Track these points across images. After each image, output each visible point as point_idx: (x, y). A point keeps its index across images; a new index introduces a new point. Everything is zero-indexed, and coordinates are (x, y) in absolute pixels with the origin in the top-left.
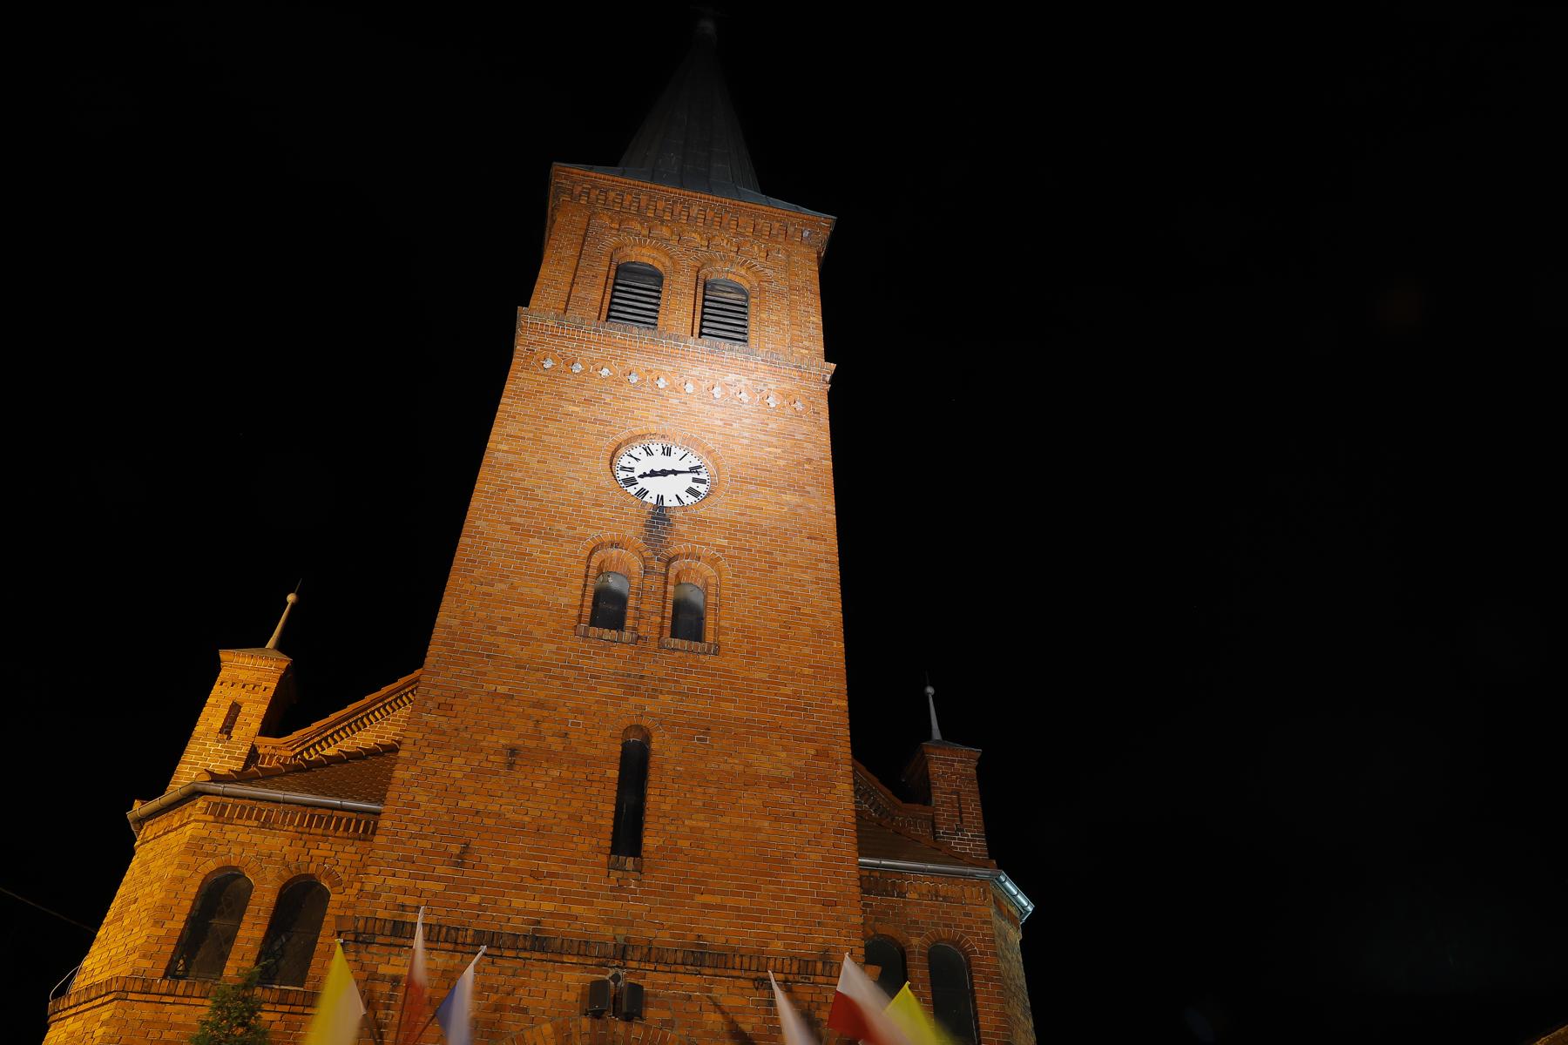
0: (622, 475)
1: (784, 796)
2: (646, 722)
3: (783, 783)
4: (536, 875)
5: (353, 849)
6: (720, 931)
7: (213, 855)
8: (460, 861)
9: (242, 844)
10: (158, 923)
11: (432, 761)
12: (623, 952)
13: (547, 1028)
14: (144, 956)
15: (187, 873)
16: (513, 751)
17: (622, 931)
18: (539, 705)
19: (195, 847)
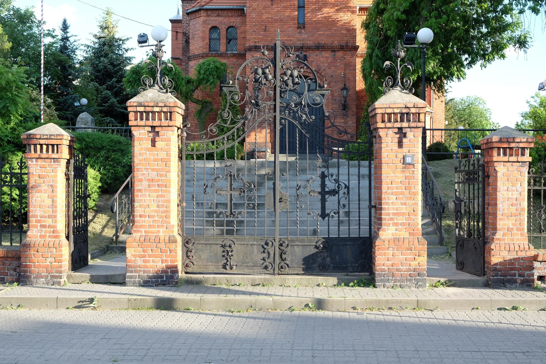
5: (239, 18)
6: (323, 40)
7: (209, 24)
8: (265, 30)
9: (214, 20)
10: (203, 41)
12: (302, 48)
14: (204, 49)
15: (205, 29)
19: (204, 22)
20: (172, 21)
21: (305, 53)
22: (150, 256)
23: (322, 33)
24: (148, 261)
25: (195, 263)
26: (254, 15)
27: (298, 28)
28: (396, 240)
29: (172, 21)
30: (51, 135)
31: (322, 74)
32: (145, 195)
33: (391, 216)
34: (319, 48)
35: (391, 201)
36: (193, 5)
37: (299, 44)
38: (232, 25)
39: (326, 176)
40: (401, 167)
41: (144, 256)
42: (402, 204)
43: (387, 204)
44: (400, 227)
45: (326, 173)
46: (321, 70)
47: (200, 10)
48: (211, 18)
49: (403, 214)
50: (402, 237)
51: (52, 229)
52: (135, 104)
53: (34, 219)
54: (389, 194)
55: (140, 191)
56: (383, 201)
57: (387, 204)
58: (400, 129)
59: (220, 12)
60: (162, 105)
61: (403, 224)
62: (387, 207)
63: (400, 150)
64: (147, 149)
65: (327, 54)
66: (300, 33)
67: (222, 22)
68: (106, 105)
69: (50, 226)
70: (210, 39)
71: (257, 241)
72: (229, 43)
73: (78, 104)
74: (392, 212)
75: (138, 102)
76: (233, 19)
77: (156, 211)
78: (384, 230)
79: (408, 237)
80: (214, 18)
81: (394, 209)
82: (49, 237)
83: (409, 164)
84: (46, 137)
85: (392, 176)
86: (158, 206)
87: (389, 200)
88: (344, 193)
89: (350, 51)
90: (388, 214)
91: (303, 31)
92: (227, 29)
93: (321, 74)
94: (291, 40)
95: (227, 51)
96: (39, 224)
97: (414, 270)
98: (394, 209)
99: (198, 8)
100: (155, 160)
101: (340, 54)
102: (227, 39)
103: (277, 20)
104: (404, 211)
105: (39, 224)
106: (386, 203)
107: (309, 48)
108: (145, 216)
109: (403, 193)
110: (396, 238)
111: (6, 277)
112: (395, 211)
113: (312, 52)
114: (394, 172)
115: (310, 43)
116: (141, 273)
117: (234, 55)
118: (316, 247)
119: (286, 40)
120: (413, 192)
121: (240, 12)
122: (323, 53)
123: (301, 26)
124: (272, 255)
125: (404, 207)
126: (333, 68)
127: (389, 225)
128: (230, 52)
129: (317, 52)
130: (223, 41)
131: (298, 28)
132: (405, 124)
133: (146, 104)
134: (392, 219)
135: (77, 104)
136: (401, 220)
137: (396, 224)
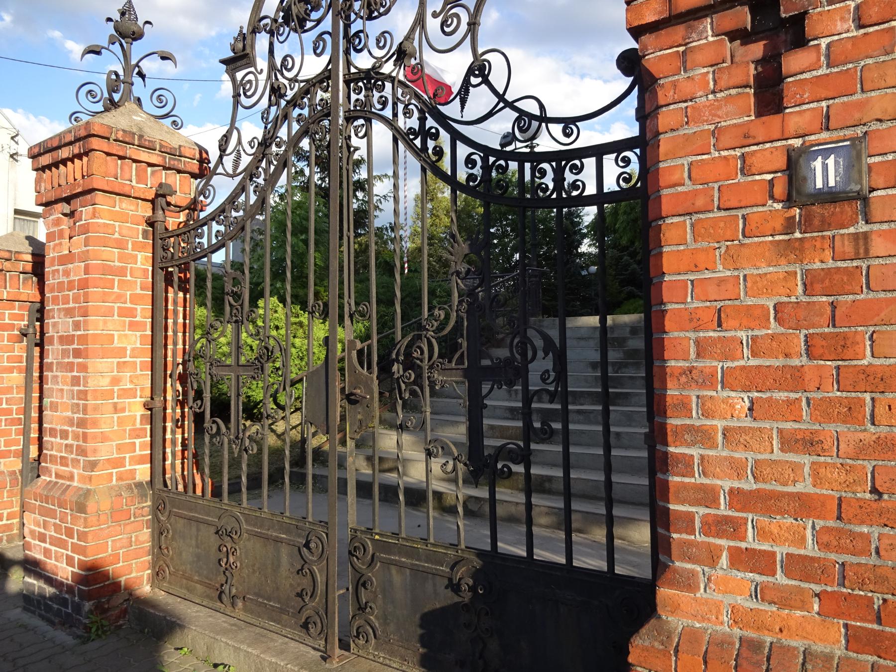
33: (723, 510)
35: (720, 424)
40: (778, 224)
42: (789, 442)
43: (704, 437)
44: (780, 578)
50: (798, 643)
54: (708, 381)
56: (673, 422)
57: (704, 437)
62: (695, 452)
63: (774, 120)
68: (627, 272)
71: (288, 531)
73: (586, 273)
74: (727, 484)
78: (689, 583)
79: (839, 651)
81: (737, 469)
83: (830, 197)
85: (721, 281)
87: (707, 414)
90: (708, 497)
98: (737, 469)
104: (804, 486)
106: (690, 429)
110: (754, 646)
112: (749, 485)
114: (731, 258)
118: (455, 587)
120: (865, 371)
124: (321, 587)
125: (806, 460)
127: (713, 561)
134: (733, 528)
135: (584, 273)
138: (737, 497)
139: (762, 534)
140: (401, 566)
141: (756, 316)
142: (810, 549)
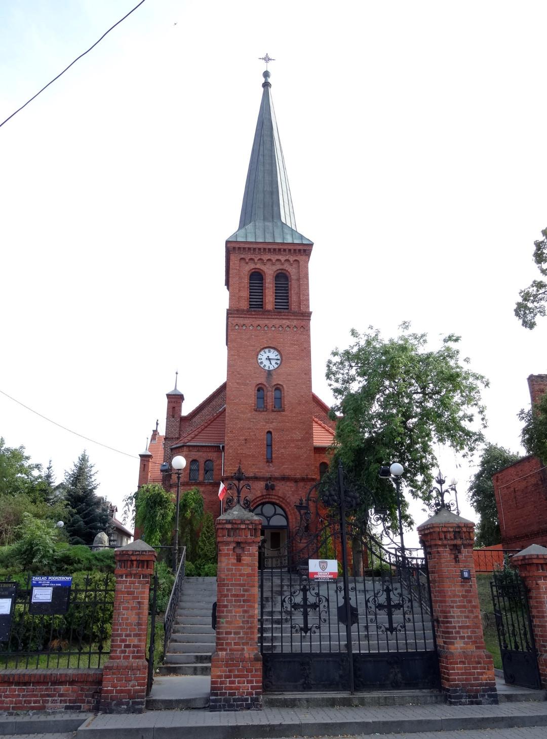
0: (259, 361)
1: (299, 443)
2: (271, 430)
3: (298, 440)
4: (253, 465)
6: (288, 473)
7: (190, 458)
9: (195, 455)
11: (231, 444)
12: (270, 478)
13: (259, 492)
14: (185, 478)
16: (246, 440)
17: (270, 474)
18: (248, 429)
20: (140, 455)
21: (273, 483)
22: (236, 676)
23: (286, 466)
24: (233, 682)
25: (274, 683)
26: (231, 451)
27: (267, 462)
28: (465, 655)
29: (140, 455)
30: (143, 551)
31: (288, 501)
32: (230, 611)
34: (284, 479)
36: (176, 442)
37: (268, 475)
38: (209, 458)
39: (391, 591)
40: (460, 581)
41: (229, 677)
43: (453, 617)
45: (390, 588)
46: (287, 497)
47: (183, 446)
48: (192, 453)
49: (468, 627)
51: (136, 649)
52: (224, 522)
53: (119, 638)
55: (226, 606)
57: (453, 617)
58: (455, 546)
59: (200, 448)
60: (248, 522)
61: (469, 637)
62: (452, 620)
64: (233, 564)
65: (292, 484)
66: (268, 466)
67: (201, 456)
69: (135, 646)
70: (190, 470)
72: (206, 473)
74: (457, 625)
75: (227, 520)
76: (210, 454)
77: (242, 628)
80: (194, 453)
81: (459, 622)
82: (134, 657)
84: (138, 553)
86: (243, 622)
88: (408, 607)
89: (310, 481)
90: (455, 627)
91: (271, 464)
92: (205, 462)
93: (286, 501)
94: (261, 472)
95: (204, 479)
96: (123, 644)
97: (487, 684)
98: (459, 622)
99: (181, 445)
100: (241, 575)
101: (302, 484)
102: (205, 470)
103: (249, 455)
104: (468, 624)
105: (123, 644)
106: (451, 616)
107: (276, 479)
108: (230, 633)
109: (464, 607)
111: (82, 705)
112: (460, 625)
113: (278, 482)
115: (277, 475)
116: (227, 696)
117: (211, 483)
119: (258, 472)
121: (219, 449)
122: (288, 483)
123: (269, 460)
125: (467, 620)
126: (296, 495)
127: (456, 639)
128: (207, 481)
129: (283, 483)
130: (202, 472)
131: (267, 462)
132: (459, 542)
133: (234, 522)
134: (458, 632)
136: (466, 633)
137: (462, 638)
138: (460, 627)
139: (463, 633)
140: (370, 661)
141: (458, 596)
142: (469, 634)
